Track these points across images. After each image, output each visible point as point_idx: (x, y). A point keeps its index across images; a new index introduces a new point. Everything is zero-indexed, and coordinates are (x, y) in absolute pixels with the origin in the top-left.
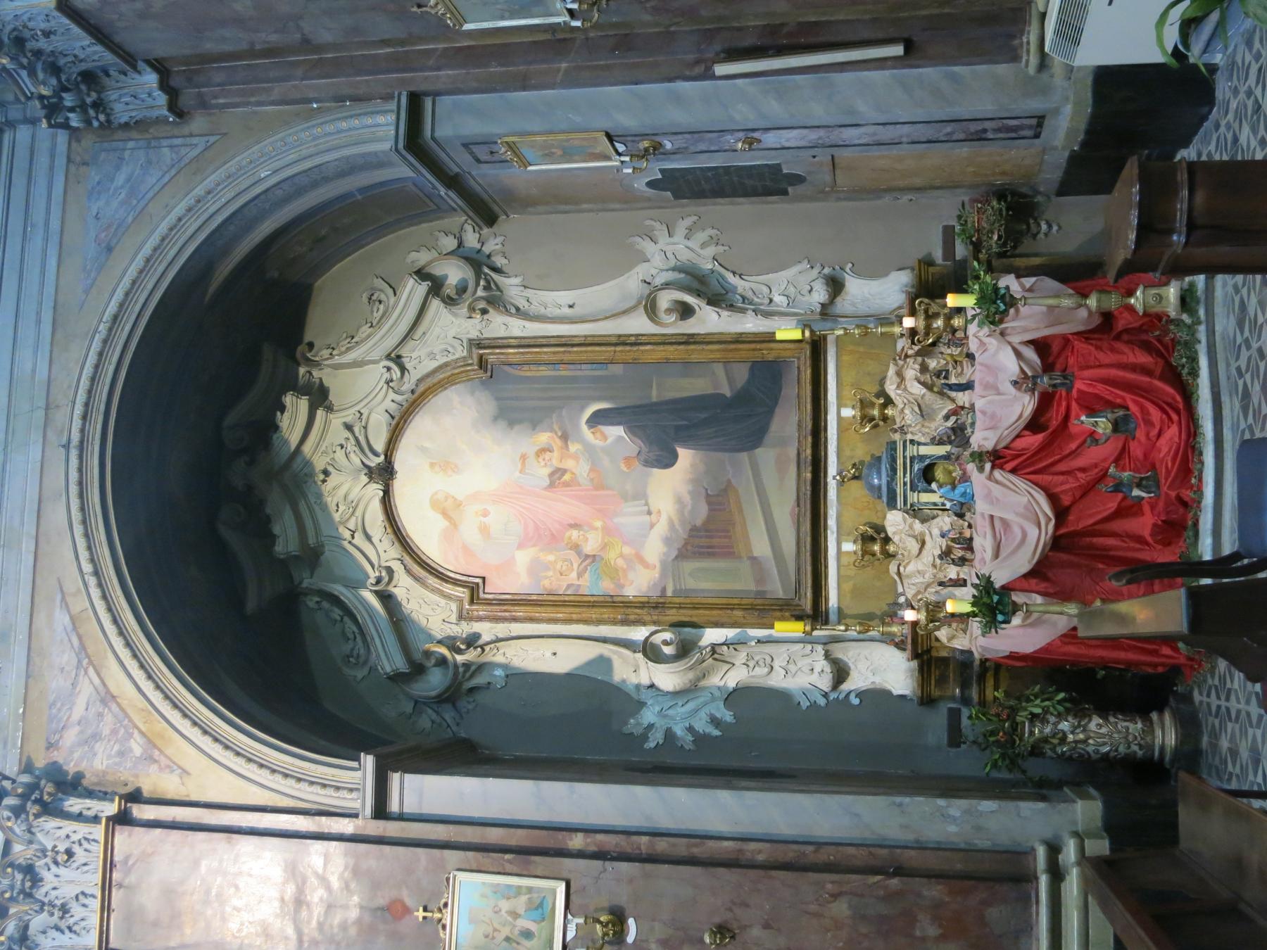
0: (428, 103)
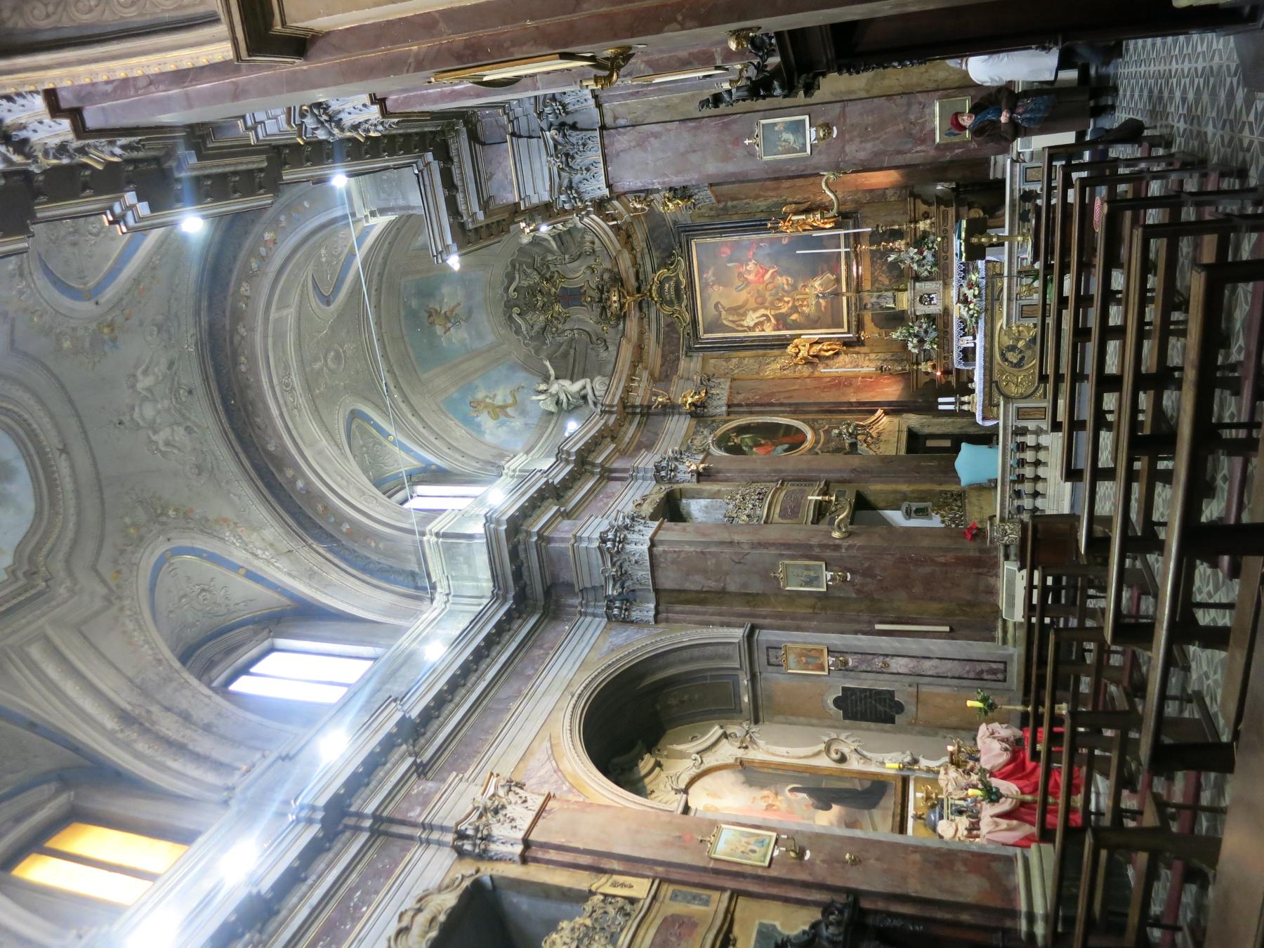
0: (757, 631)
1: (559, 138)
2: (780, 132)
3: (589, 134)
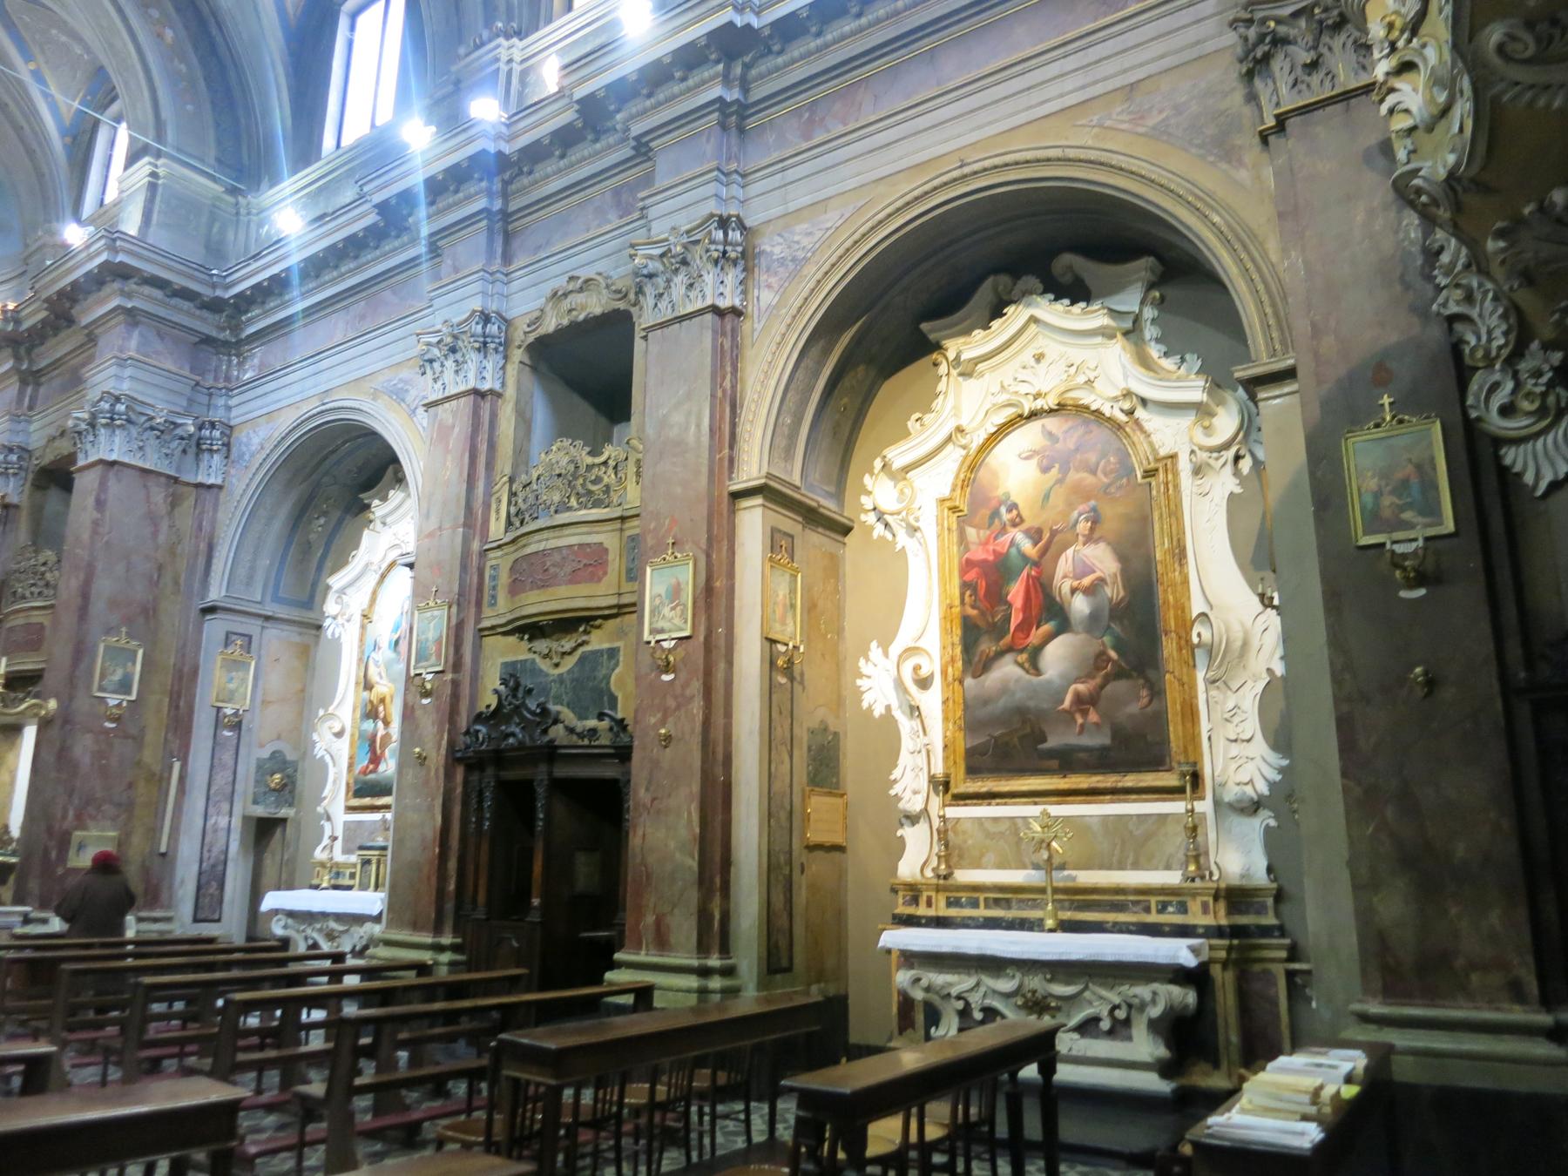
1: (179, 431)
2: (125, 666)
3: (174, 464)
